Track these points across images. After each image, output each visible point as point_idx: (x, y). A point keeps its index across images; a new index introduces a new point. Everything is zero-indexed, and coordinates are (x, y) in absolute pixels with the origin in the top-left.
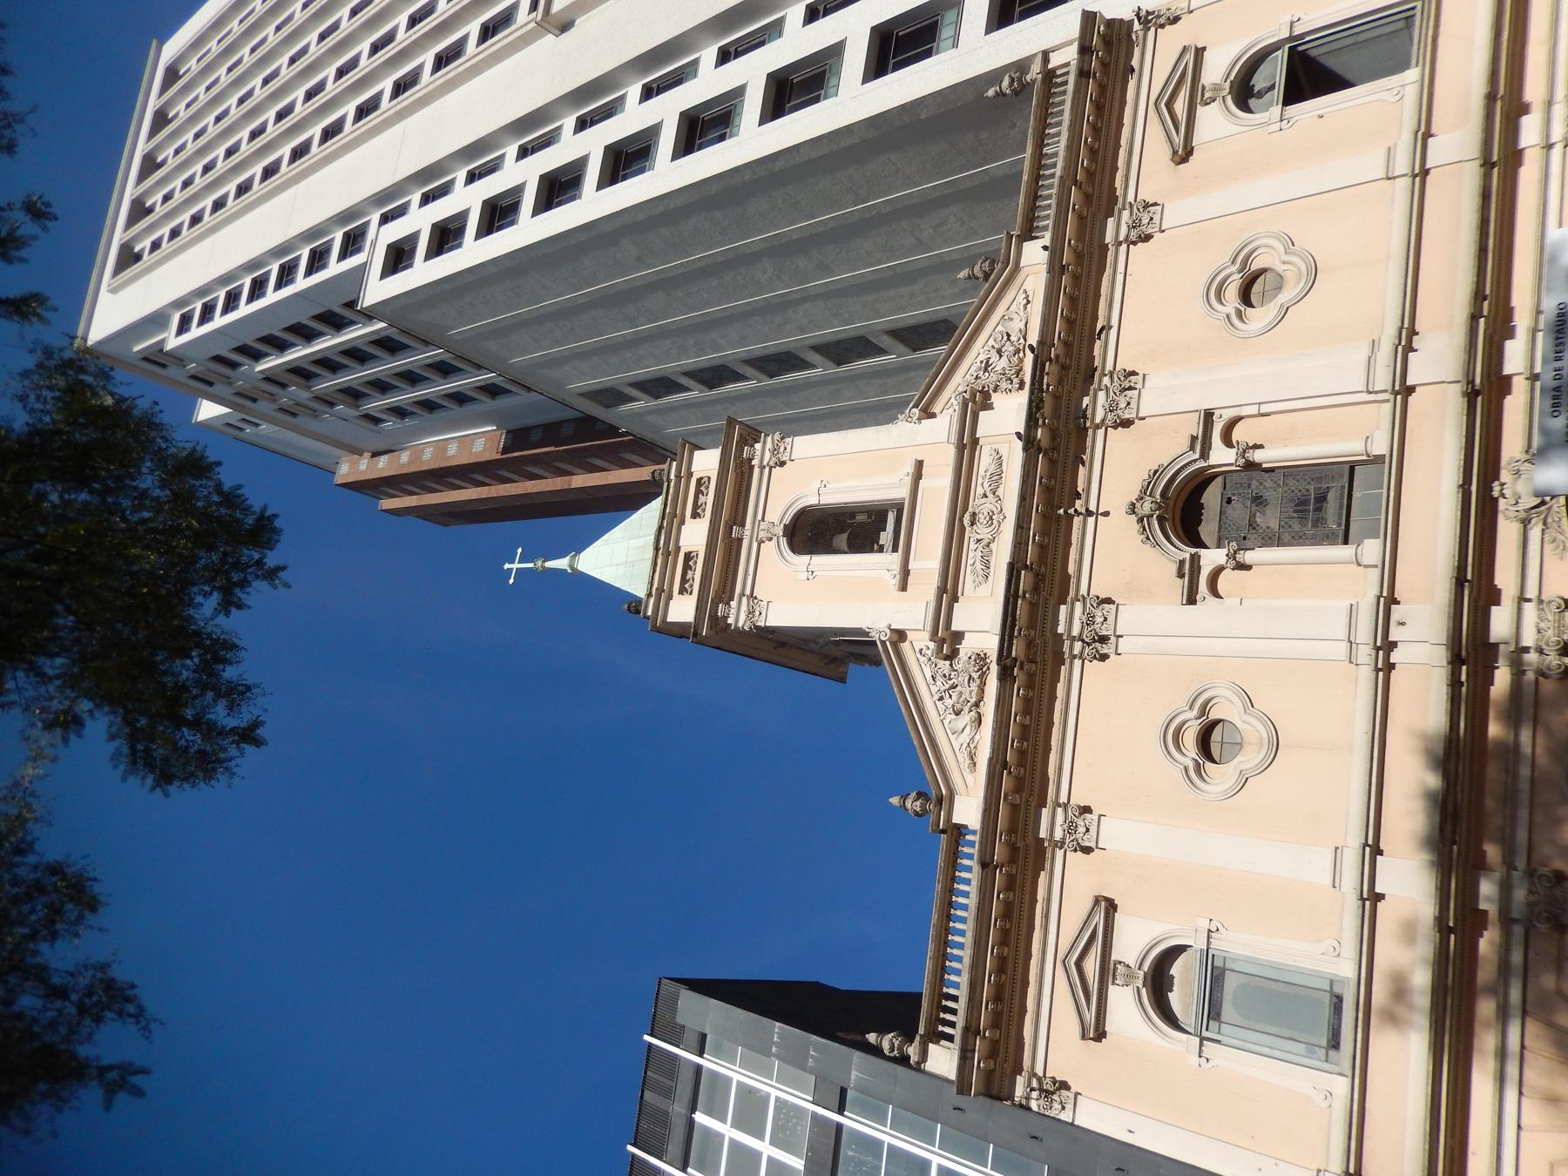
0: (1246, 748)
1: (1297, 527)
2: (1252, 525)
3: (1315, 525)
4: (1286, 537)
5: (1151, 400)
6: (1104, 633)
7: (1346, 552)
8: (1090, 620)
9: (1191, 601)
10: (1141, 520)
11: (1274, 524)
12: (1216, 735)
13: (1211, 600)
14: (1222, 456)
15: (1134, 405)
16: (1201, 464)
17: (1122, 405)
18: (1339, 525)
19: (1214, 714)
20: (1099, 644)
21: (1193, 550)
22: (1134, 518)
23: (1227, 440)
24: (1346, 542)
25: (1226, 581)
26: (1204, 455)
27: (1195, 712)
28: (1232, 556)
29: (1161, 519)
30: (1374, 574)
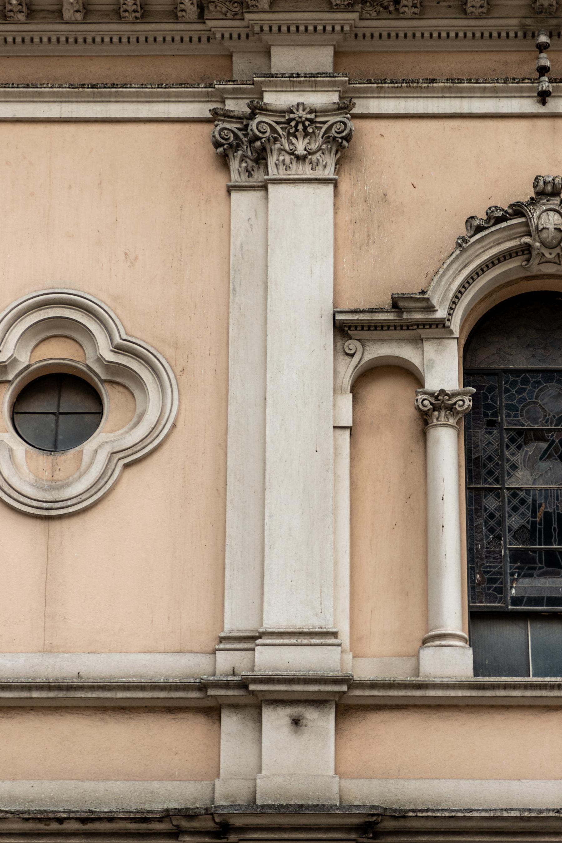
0: (42, 461)
1: (514, 521)
2: (521, 437)
3: (516, 555)
4: (491, 503)
6: (272, 161)
7: (452, 611)
8: (297, 123)
9: (343, 330)
10: (518, 210)
11: (522, 479)
12: (71, 401)
13: (348, 370)
18: (516, 601)
19: (111, 398)
21: (455, 325)
22: (526, 193)
24: (476, 616)
25: (385, 395)
27: (109, 356)
28: (441, 402)
29: (527, 249)
30: (400, 671)
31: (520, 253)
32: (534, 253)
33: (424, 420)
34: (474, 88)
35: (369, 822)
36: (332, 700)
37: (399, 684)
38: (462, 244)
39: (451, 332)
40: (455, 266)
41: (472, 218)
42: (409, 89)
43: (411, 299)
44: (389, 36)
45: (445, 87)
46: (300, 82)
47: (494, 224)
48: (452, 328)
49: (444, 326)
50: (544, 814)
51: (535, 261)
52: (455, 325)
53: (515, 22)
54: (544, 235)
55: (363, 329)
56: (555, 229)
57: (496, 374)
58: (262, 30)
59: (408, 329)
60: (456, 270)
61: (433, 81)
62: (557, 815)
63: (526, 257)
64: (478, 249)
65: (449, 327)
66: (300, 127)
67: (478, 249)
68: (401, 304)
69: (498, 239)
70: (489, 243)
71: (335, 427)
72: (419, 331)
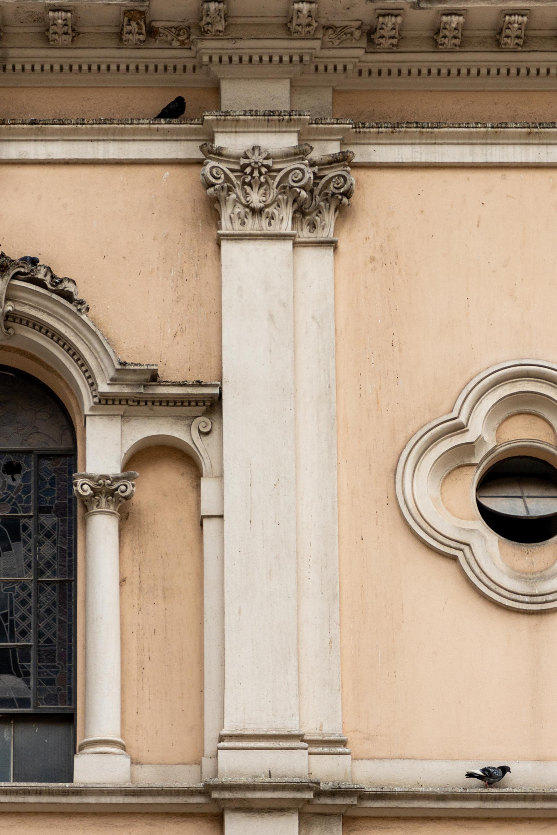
5: (259, 270)
14: (103, 448)
15: (253, 225)
16: (88, 402)
17: (256, 198)
23: (144, 456)
26: (105, 401)
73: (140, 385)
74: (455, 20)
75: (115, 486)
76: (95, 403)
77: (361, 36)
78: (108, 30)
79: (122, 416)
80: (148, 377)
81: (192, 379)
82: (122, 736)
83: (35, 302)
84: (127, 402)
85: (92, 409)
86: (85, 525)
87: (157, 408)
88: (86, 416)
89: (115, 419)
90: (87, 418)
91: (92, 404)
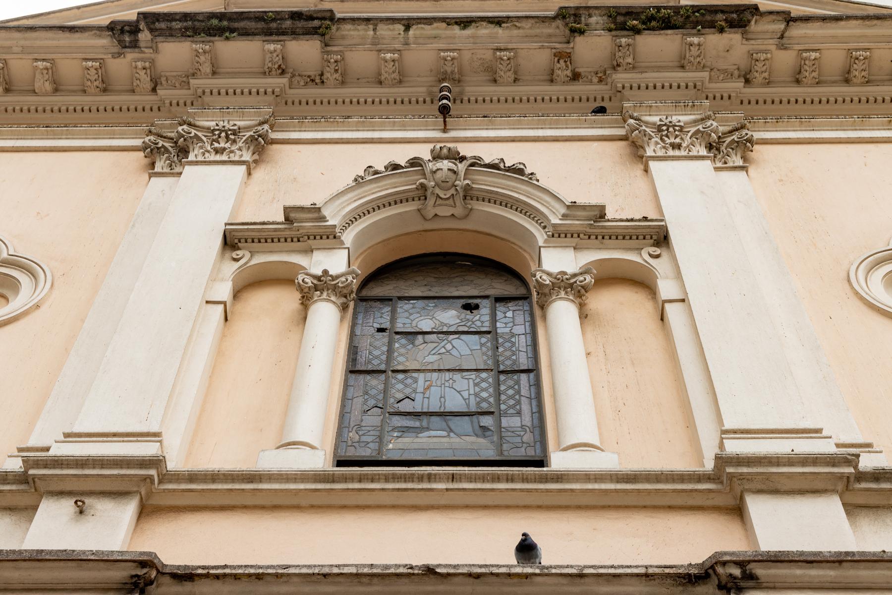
16: (541, 237)
20: (169, 152)
31: (416, 199)
32: (429, 193)
33: (306, 301)
34: (384, 122)
35: (137, 576)
36: (135, 492)
37: (224, 475)
38: (359, 181)
39: (342, 243)
40: (350, 195)
41: (370, 167)
42: (327, 124)
43: (302, 209)
44: (315, 103)
45: (359, 122)
46: (228, 113)
47: (393, 170)
48: (342, 238)
49: (335, 237)
50: (392, 571)
51: (431, 201)
52: (348, 237)
53: (423, 89)
54: (439, 175)
55: (253, 242)
56: (449, 170)
57: (391, 300)
58: (204, 93)
59: (299, 241)
60: (351, 198)
61: (349, 117)
62: (410, 571)
63: (422, 202)
64: (375, 188)
65: (340, 237)
66: (223, 134)
67: (375, 188)
68: (292, 215)
69: (395, 183)
70: (385, 185)
71: (207, 302)
72: (310, 242)
73: (590, 220)
74: (813, 55)
75: (572, 281)
76: (548, 236)
77: (739, 76)
78: (542, 78)
79: (575, 248)
80: (597, 213)
81: (638, 216)
82: (601, 444)
83: (490, 182)
84: (579, 236)
85: (545, 241)
86: (544, 317)
87: (607, 241)
88: (540, 247)
89: (568, 250)
90: (542, 249)
91: (546, 237)
